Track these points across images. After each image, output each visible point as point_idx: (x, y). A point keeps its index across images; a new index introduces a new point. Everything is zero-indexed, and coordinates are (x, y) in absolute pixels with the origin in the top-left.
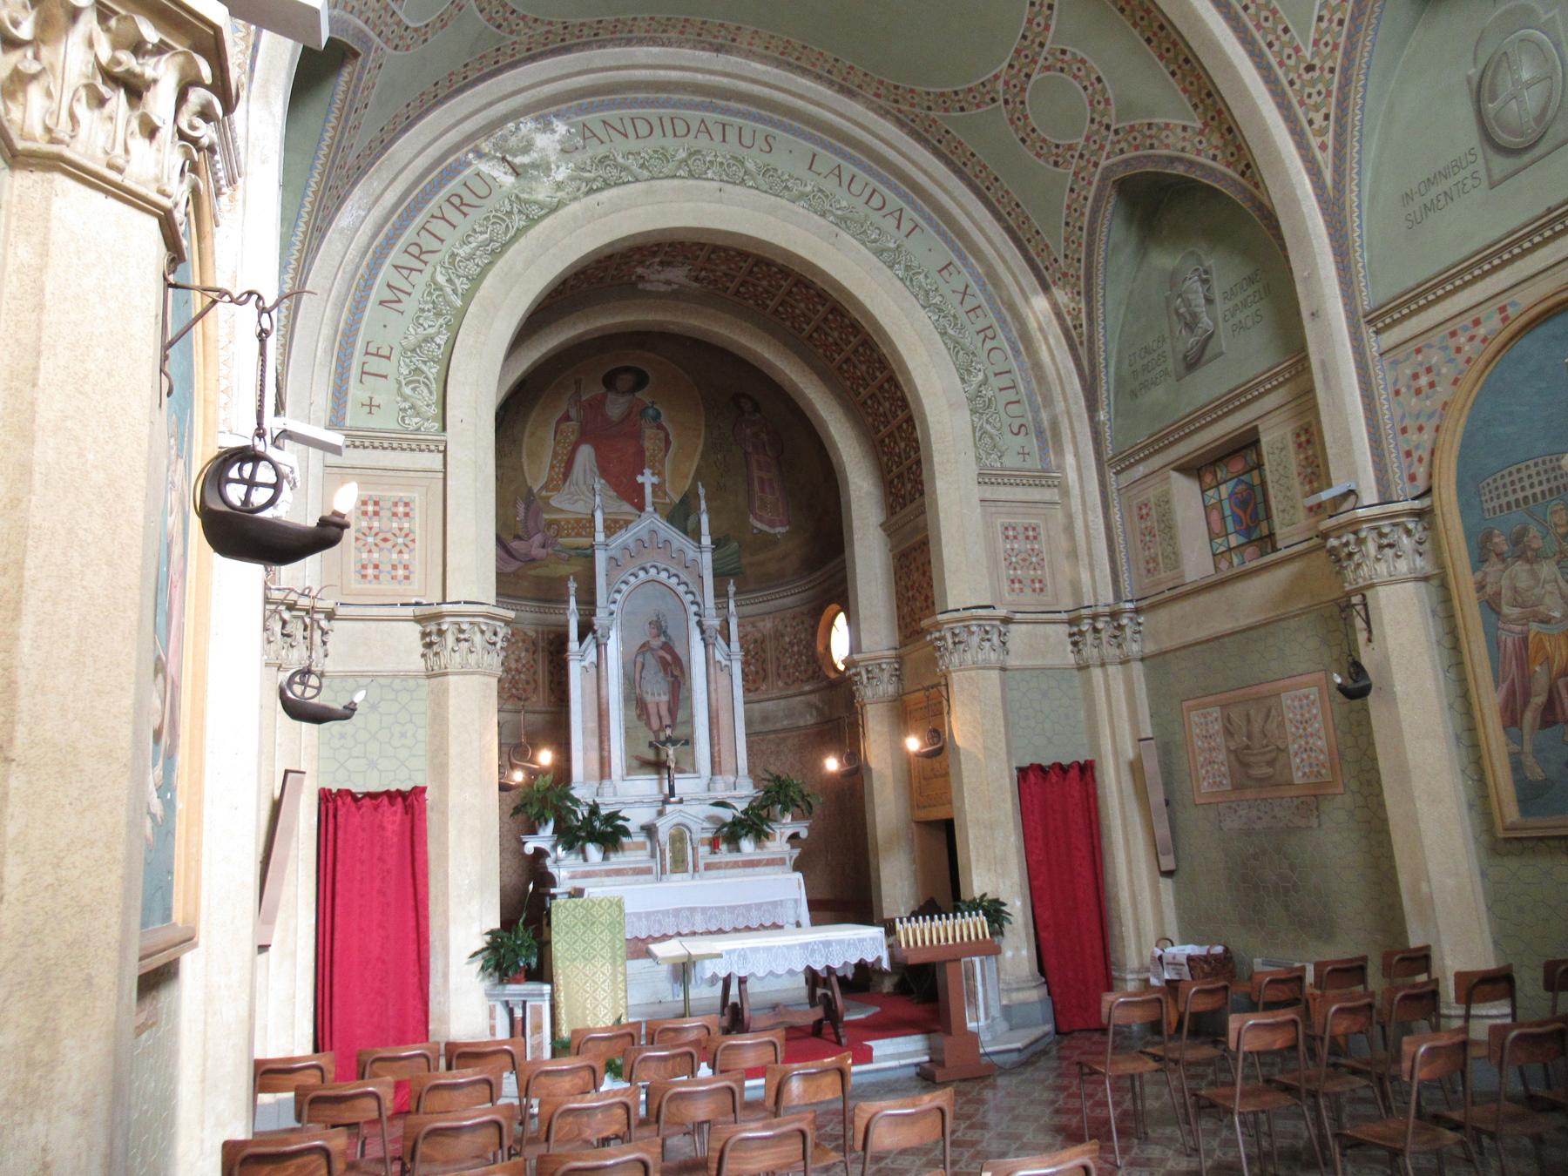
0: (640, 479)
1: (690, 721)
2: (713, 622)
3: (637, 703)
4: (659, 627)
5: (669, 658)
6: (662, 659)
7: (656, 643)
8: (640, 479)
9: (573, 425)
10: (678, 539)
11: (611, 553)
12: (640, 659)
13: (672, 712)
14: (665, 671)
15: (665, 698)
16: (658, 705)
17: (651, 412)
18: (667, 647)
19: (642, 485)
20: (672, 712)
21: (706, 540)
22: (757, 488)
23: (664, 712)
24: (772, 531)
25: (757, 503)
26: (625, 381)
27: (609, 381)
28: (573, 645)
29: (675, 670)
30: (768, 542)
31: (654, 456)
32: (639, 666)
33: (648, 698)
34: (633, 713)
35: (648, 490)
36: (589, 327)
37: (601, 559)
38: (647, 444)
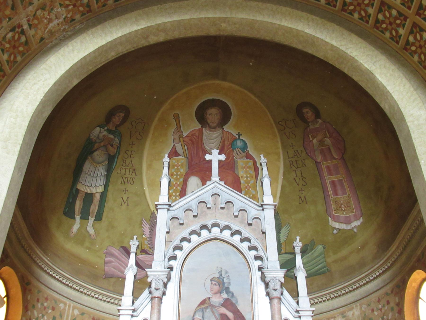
0: (208, 157)
2: (277, 274)
4: (221, 284)
5: (230, 315)
7: (217, 300)
8: (208, 157)
9: (182, 160)
10: (239, 200)
11: (172, 213)
17: (239, 143)
18: (229, 304)
19: (210, 161)
21: (268, 199)
22: (331, 193)
24: (348, 227)
25: (333, 206)
26: (213, 115)
27: (201, 116)
28: (127, 299)
30: (346, 238)
31: (247, 182)
35: (215, 167)
36: (149, 24)
37: (163, 218)
38: (241, 173)
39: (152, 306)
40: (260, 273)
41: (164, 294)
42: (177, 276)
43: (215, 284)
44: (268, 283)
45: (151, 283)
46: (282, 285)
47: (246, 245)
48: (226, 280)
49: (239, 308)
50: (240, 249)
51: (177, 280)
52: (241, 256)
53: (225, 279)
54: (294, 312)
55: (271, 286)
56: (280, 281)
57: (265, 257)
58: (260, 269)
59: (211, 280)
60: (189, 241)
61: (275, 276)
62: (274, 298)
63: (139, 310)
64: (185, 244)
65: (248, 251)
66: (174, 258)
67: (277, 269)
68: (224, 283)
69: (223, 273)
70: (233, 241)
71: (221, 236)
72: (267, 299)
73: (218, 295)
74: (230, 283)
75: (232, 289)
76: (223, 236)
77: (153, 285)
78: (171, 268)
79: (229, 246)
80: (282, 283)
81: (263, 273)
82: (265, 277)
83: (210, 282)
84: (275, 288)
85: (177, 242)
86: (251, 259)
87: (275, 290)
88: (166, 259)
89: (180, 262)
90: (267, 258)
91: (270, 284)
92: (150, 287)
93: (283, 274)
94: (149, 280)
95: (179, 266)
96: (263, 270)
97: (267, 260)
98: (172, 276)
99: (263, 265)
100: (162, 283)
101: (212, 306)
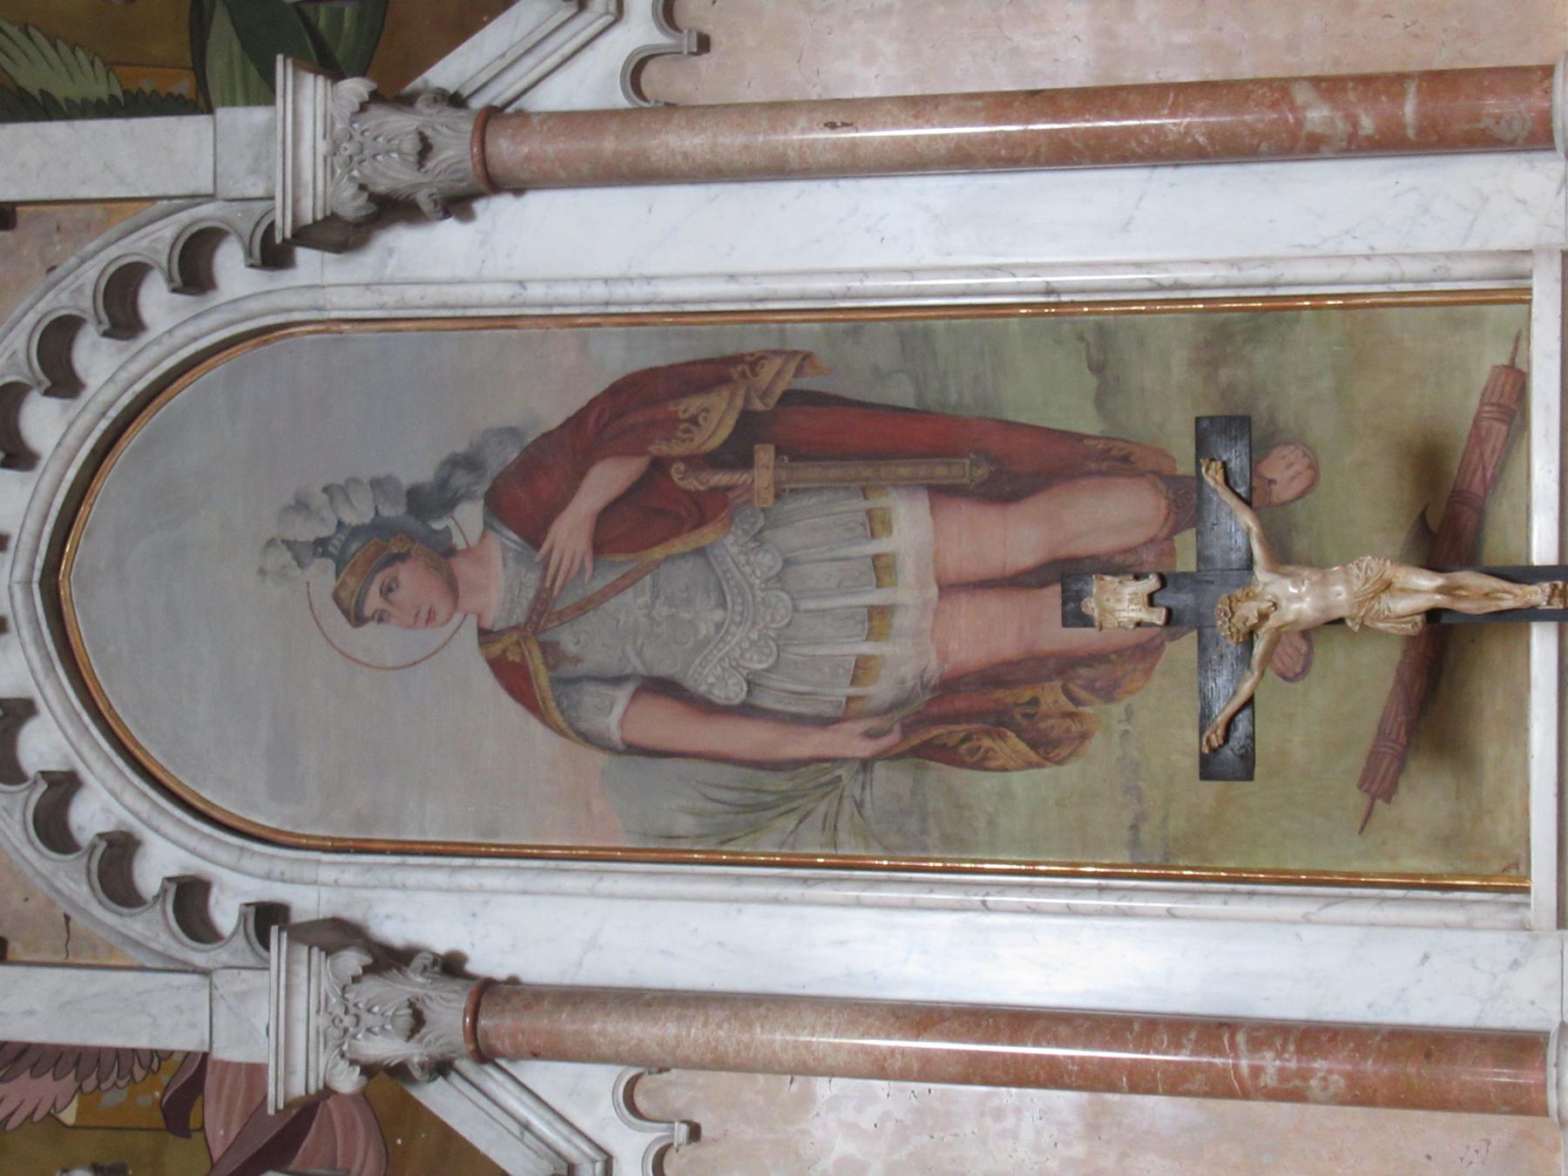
1: (1096, 330)
3: (947, 759)
4: (380, 551)
5: (606, 481)
6: (619, 531)
7: (498, 581)
12: (612, 713)
13: (1005, 464)
14: (705, 510)
15: (911, 526)
16: (949, 588)
18: (525, 492)
20: (1005, 464)
23: (1019, 536)
29: (707, 430)
32: (663, 724)
33: (906, 661)
34: (1018, 790)
39: (536, 1055)
40: (303, 255)
41: (451, 966)
42: (327, 874)
43: (386, 591)
44: (373, 198)
45: (370, 1070)
46: (391, 94)
47: (95, 357)
48: (359, 513)
49: (553, 415)
50: (126, 400)
51: (349, 876)
52: (182, 397)
53: (351, 519)
54: (586, 16)
55: (395, 175)
56: (363, 107)
57: (184, 217)
58: (273, 255)
59: (357, 618)
60: (64, 785)
61: (323, 147)
62: (484, 161)
63: (563, 1146)
64: (91, 815)
65: (144, 339)
66: (189, 896)
67: (270, 130)
68: (379, 528)
69: (305, 531)
70: (64, 452)
71: (27, 539)
72: (496, 211)
73: (463, 568)
74: (377, 484)
75: (418, 470)
76: (32, 525)
77: (387, 1047)
78: (267, 918)
79: (108, 483)
80: (376, 97)
81: (305, 235)
82: (332, 219)
83: (370, 629)
84: (410, 145)
85: (70, 881)
86: (206, 323)
87: (425, 149)
88: (200, 956)
89: (223, 855)
90: (196, 199)
91: (382, 186)
92: (400, 1071)
93: (314, 88)
94: (347, 1081)
95: (248, 863)
96: (284, 230)
97: (211, 197)
98: (326, 911)
99: (246, 227)
100: (374, 987)
101: (543, 611)
